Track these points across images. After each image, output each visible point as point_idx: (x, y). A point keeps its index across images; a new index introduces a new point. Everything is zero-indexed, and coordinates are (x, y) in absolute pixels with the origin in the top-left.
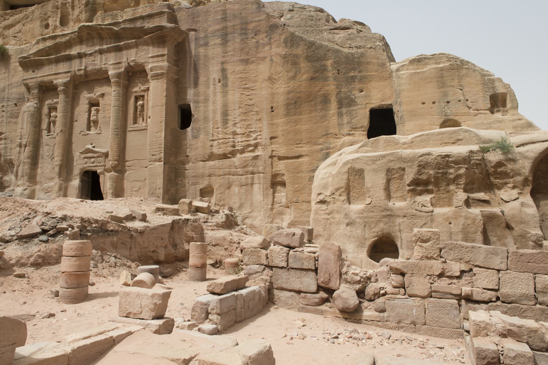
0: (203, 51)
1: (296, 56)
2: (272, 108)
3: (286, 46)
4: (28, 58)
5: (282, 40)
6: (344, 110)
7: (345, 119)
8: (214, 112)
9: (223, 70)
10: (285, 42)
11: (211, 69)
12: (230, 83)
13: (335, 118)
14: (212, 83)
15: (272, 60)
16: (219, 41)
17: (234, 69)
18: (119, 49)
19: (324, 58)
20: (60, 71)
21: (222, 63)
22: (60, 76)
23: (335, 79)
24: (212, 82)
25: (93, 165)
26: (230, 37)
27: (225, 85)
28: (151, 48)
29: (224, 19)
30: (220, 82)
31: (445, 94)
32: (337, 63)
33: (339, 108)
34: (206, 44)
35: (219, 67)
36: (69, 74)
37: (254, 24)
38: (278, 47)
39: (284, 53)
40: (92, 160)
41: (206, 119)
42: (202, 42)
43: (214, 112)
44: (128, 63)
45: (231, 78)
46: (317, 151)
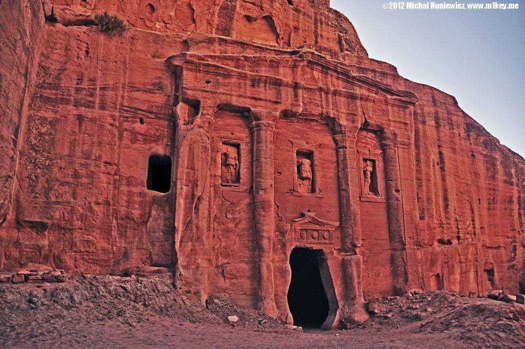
0: (421, 128)
1: (496, 159)
2: (479, 200)
3: (486, 148)
4: (203, 60)
5: (481, 141)
8: (437, 195)
9: (441, 153)
12: (446, 168)
14: (432, 164)
15: (473, 156)
16: (433, 123)
17: (446, 153)
20: (262, 96)
21: (439, 146)
22: (262, 103)
23: (517, 185)
24: (432, 164)
25: (316, 241)
26: (442, 122)
27: (442, 169)
30: (438, 164)
33: (519, 209)
34: (424, 122)
35: (437, 150)
36: (278, 106)
39: (485, 153)
40: (315, 234)
41: (429, 199)
42: (420, 119)
43: (437, 195)
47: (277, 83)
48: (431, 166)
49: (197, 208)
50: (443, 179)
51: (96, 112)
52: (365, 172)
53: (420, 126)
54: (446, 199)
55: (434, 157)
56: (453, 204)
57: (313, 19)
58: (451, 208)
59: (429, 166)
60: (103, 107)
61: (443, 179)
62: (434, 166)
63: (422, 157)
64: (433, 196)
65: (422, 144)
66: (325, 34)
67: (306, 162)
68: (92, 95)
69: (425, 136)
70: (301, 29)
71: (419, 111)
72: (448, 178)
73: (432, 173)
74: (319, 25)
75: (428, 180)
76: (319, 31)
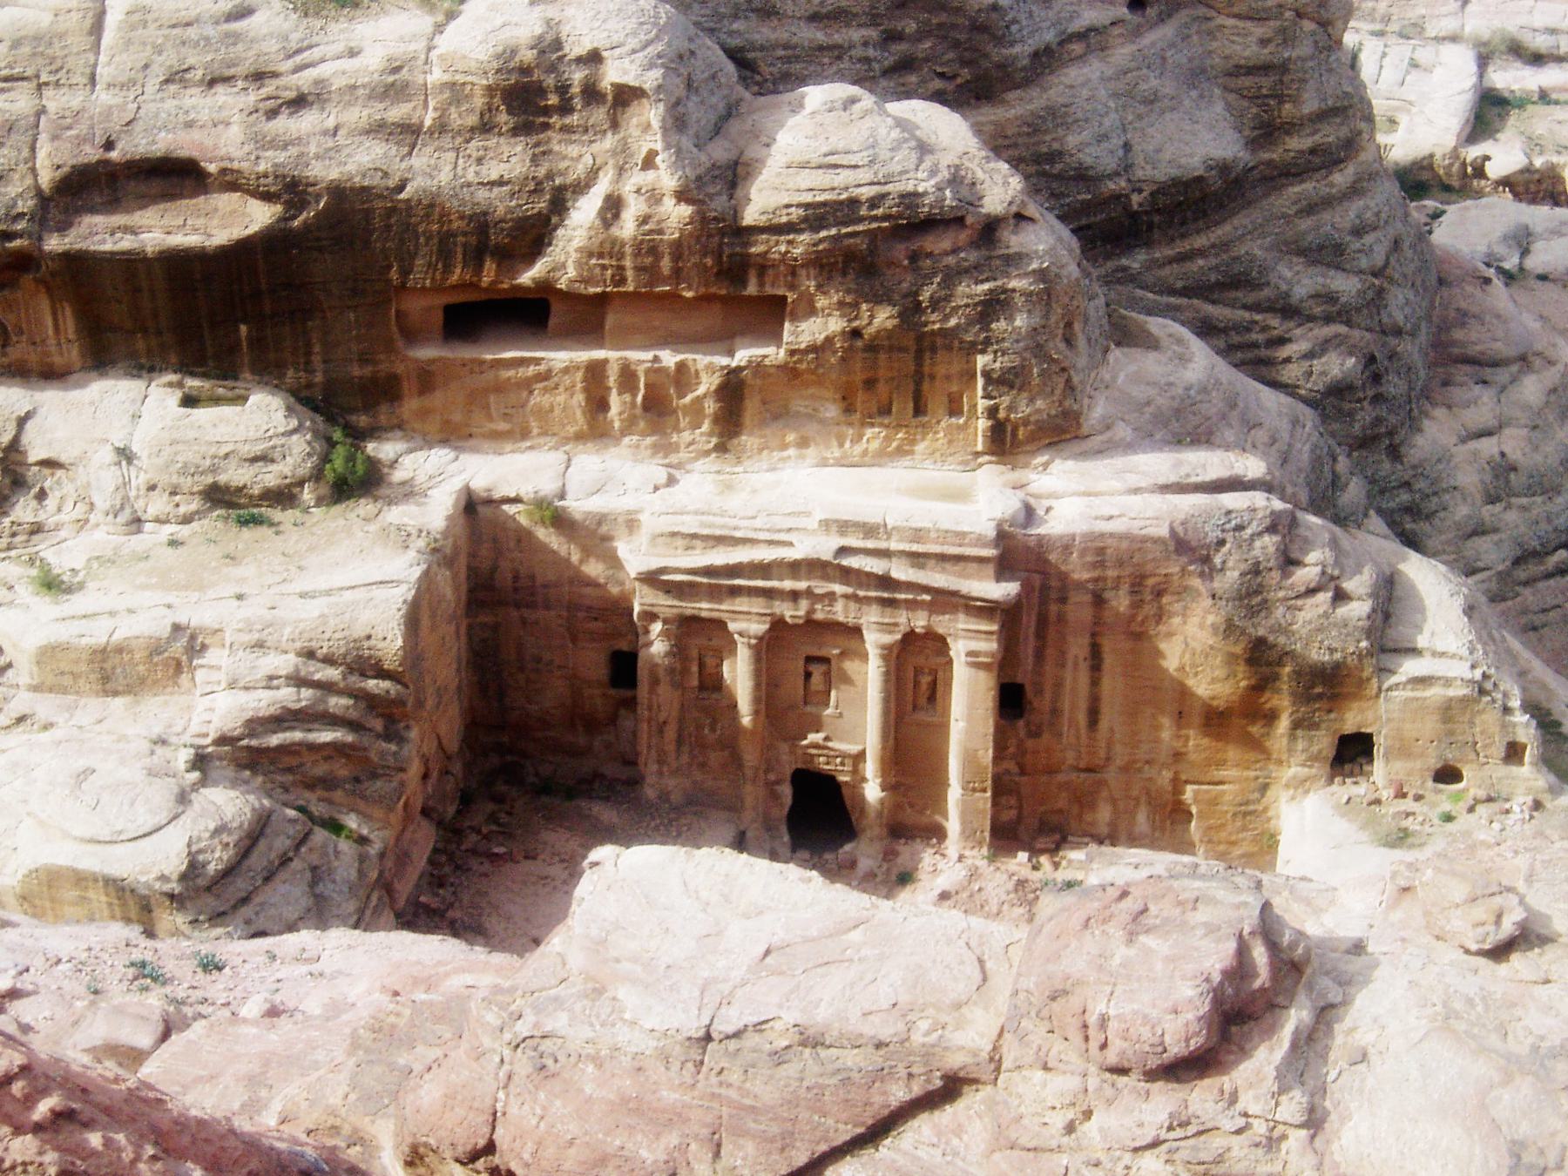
6: (1299, 733)
7: (1300, 745)
10: (1214, 627)
11: (1070, 639)
13: (1285, 741)
18: (890, 603)
19: (1280, 663)
21: (1093, 635)
28: (961, 616)
29: (1100, 564)
31: (1451, 733)
32: (1298, 674)
34: (1063, 600)
37: (1157, 579)
38: (1201, 626)
41: (1056, 712)
42: (1054, 595)
44: (913, 631)
45: (1109, 660)
46: (1247, 779)
47: (768, 594)
48: (1070, 664)
49: (661, 732)
50: (1095, 683)
51: (540, 614)
52: (916, 684)
53: (1054, 608)
54: (1094, 715)
55: (1078, 648)
56: (1109, 717)
57: (913, 348)
58: (1104, 724)
59: (1063, 666)
60: (547, 608)
61: (1095, 683)
62: (1076, 665)
63: (1050, 652)
64: (1066, 706)
65: (1052, 634)
66: (941, 370)
67: (817, 671)
68: (532, 594)
69: (1061, 619)
70: (882, 381)
71: (1054, 583)
72: (1107, 684)
73: (1068, 675)
74: (928, 355)
75: (1059, 685)
76: (926, 369)
